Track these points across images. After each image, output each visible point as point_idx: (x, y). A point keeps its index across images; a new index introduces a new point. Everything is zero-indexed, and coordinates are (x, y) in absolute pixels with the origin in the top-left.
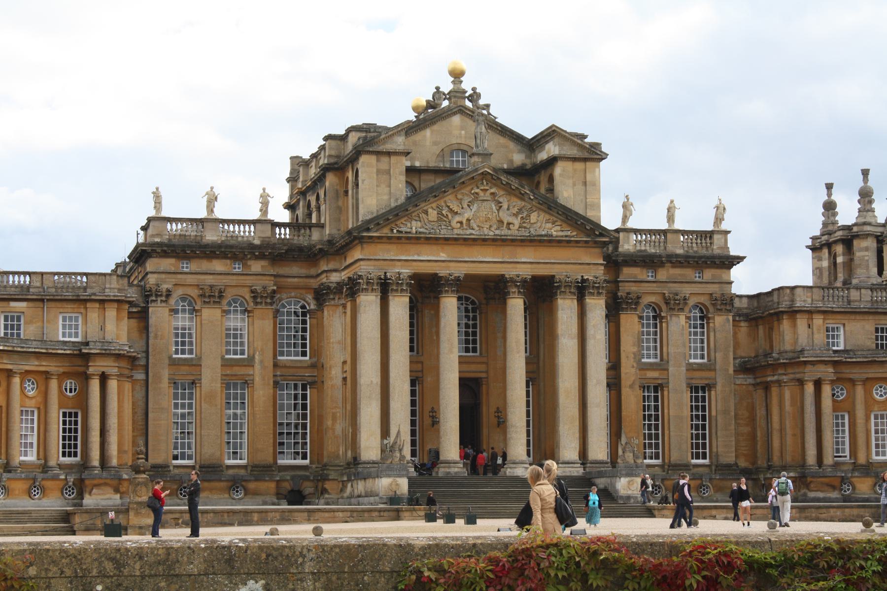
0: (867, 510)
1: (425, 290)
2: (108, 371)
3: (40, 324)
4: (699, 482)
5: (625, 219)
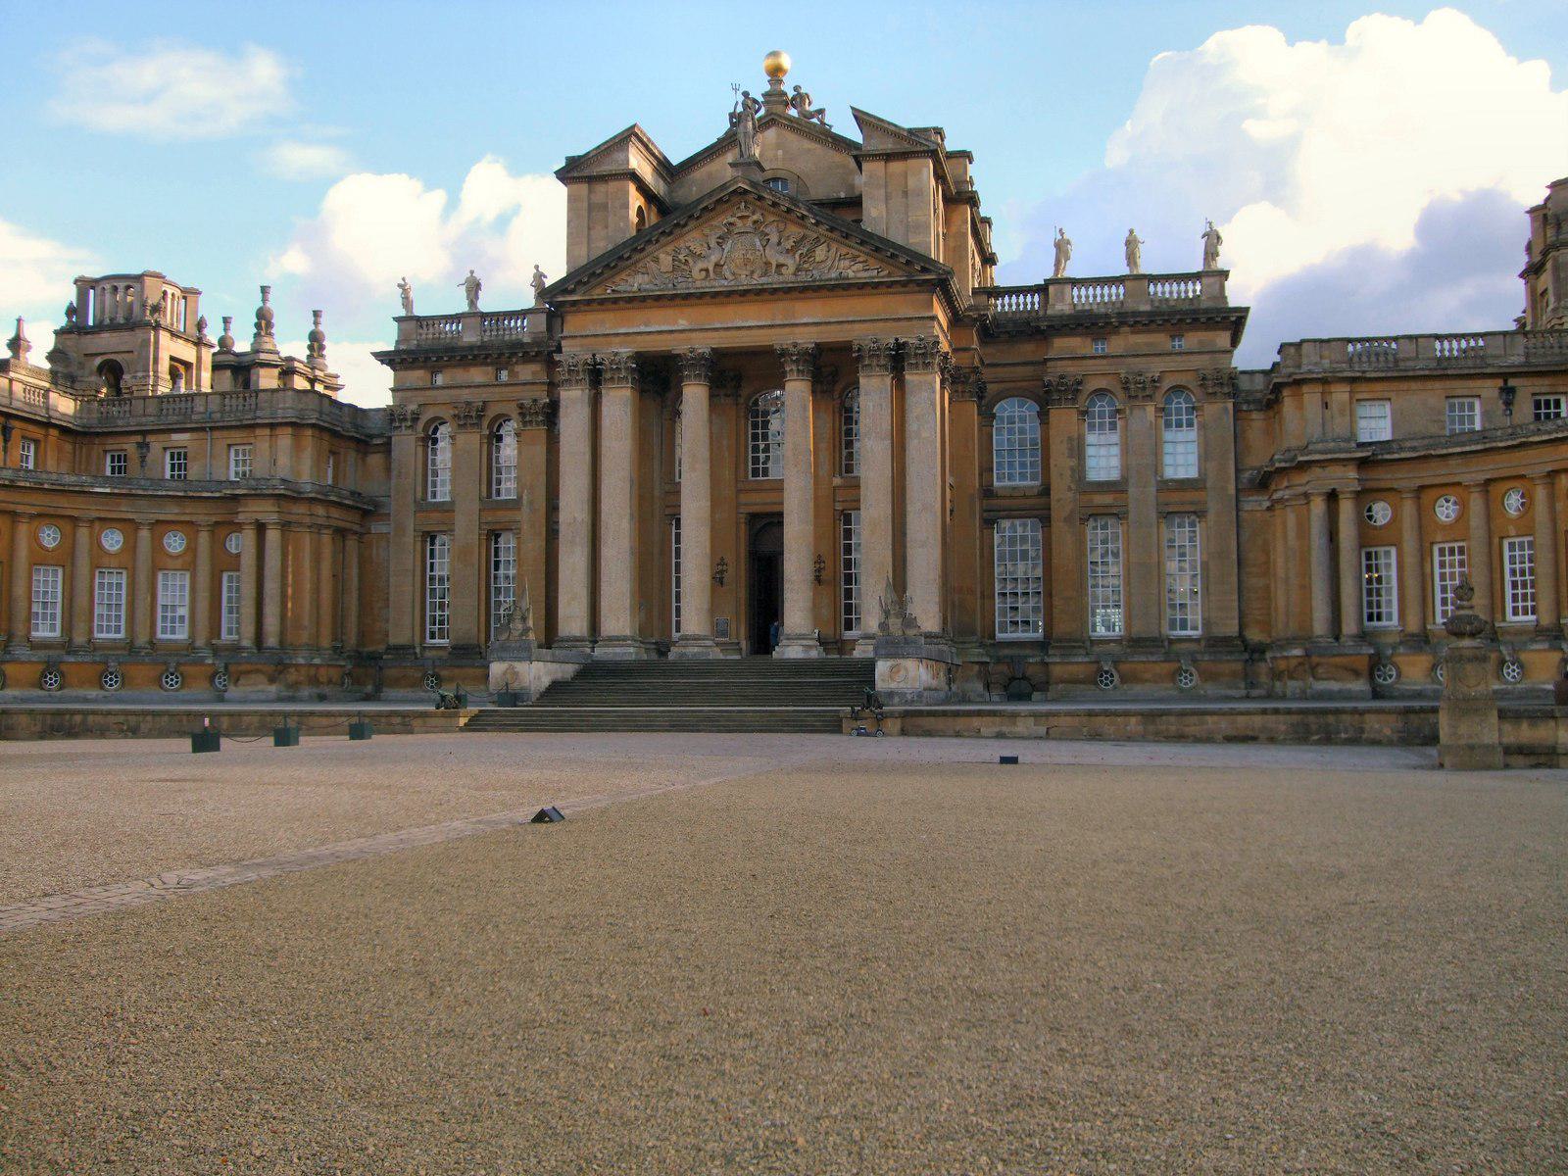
0: (1281, 718)
1: (657, 377)
4: (1177, 665)
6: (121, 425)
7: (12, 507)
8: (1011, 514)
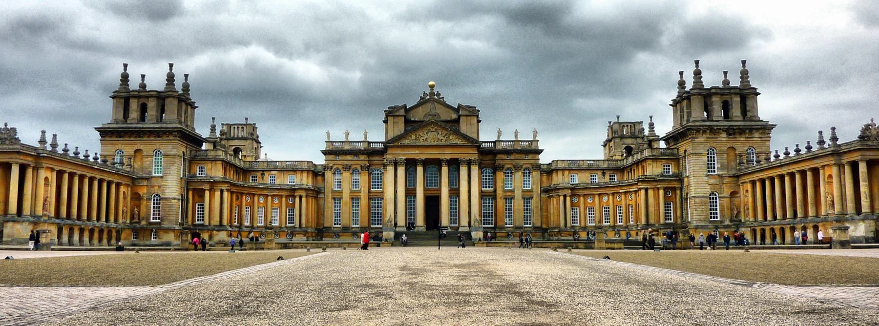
1: (411, 164)
5: (499, 137)
8: (486, 196)
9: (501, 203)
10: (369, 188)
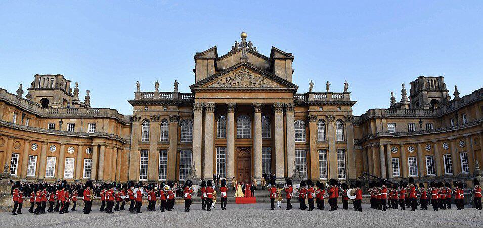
1: (221, 110)
2: (100, 144)
3: (80, 127)
5: (311, 88)
6: (54, 116)
7: (25, 137)
9: (315, 156)
10: (178, 140)
